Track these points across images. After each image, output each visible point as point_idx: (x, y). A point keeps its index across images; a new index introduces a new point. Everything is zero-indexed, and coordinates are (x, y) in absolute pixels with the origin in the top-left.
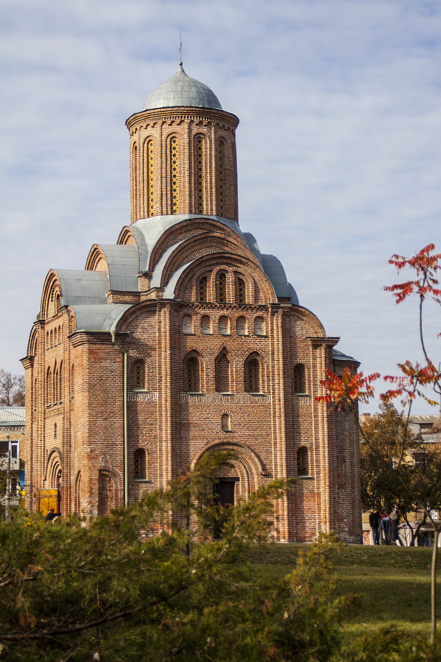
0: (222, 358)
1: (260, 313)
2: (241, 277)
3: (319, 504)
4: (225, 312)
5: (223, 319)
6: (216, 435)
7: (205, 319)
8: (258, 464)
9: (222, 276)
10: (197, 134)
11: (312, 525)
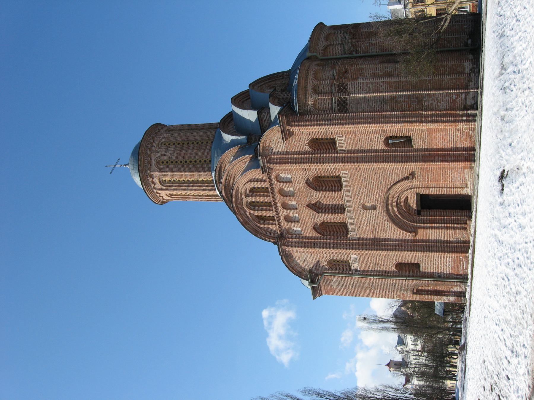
0: (317, 207)
1: (273, 178)
2: (248, 191)
3: (438, 130)
4: (279, 204)
5: (285, 206)
6: (380, 215)
7: (288, 219)
8: (402, 183)
9: (252, 205)
10: (161, 184)
11: (459, 135)
